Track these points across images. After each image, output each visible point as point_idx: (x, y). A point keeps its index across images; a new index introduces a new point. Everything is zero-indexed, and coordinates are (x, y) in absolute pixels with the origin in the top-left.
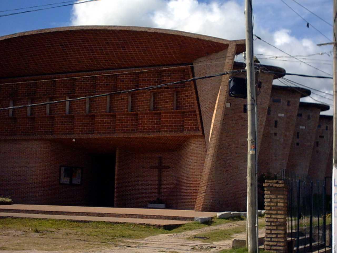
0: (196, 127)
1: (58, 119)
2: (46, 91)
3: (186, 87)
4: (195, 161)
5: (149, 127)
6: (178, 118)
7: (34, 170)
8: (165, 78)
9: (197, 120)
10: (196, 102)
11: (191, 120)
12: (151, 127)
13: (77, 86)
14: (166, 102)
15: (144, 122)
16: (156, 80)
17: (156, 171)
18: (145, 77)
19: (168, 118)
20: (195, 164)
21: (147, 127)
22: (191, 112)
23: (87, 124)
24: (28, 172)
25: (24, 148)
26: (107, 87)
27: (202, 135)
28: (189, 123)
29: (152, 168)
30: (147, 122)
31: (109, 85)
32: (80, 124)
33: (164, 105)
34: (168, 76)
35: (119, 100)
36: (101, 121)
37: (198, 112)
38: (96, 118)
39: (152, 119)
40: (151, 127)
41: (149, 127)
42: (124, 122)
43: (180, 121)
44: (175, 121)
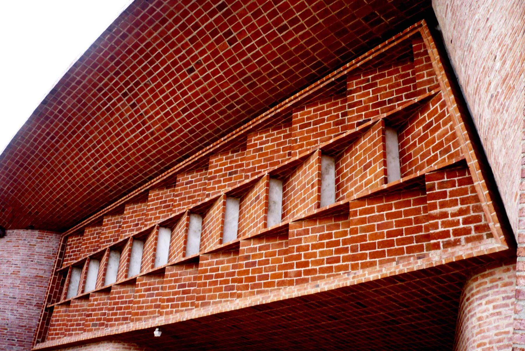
0: (477, 228)
5: (321, 262)
6: (407, 213)
8: (358, 97)
9: (476, 199)
10: (460, 127)
11: (454, 203)
12: (329, 261)
15: (307, 248)
16: (337, 116)
23: (190, 285)
27: (505, 247)
28: (444, 215)
30: (314, 247)
31: (236, 172)
33: (362, 178)
34: (365, 88)
37: (473, 163)
39: (330, 236)
40: (329, 261)
41: (321, 262)
42: (260, 263)
43: (417, 221)
44: (398, 224)
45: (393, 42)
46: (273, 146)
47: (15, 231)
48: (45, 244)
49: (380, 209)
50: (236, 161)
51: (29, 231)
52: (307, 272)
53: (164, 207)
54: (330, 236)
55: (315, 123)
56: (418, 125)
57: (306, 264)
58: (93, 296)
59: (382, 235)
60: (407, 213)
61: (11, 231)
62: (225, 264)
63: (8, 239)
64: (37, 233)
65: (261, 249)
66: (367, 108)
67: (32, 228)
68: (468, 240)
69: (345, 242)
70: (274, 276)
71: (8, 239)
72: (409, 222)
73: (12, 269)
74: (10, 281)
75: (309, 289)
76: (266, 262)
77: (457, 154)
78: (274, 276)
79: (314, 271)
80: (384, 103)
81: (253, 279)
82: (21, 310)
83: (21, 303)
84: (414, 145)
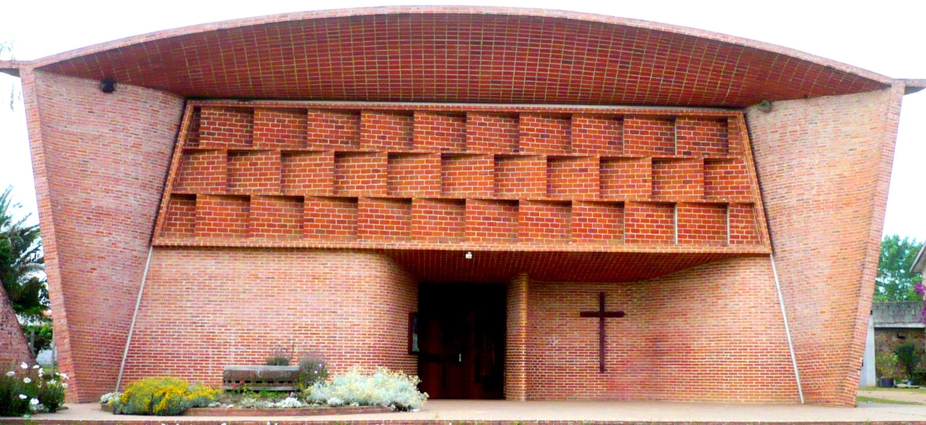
1: (420, 207)
2: (384, 138)
3: (732, 154)
4: (752, 304)
6: (709, 217)
11: (742, 222)
13: (471, 133)
15: (637, 221)
18: (637, 127)
19: (690, 216)
20: (753, 310)
21: (644, 231)
22: (743, 205)
23: (494, 219)
24: (339, 325)
25: (327, 270)
26: (543, 141)
29: (584, 315)
30: (643, 221)
31: (548, 136)
32: (479, 218)
33: (681, 187)
34: (689, 129)
35: (575, 170)
36: (532, 214)
37: (759, 207)
38: (522, 209)
42: (590, 220)
45: (720, 113)
46: (595, 132)
47: (130, 87)
48: (168, 111)
49: (695, 211)
50: (548, 126)
51: (151, 91)
52: (638, 236)
53: (437, 134)
54: (652, 216)
55: (642, 133)
56: (721, 168)
57: (638, 231)
58: (309, 200)
59: (695, 226)
60: (709, 217)
61: (122, 86)
62: (546, 213)
63: (120, 97)
64: (160, 94)
65: (590, 210)
66: (689, 143)
67: (155, 88)
68: (747, 242)
69: (662, 222)
70: (601, 231)
71: (120, 97)
72: (709, 222)
73: (132, 140)
74: (131, 156)
75: (647, 249)
76: (595, 220)
77: (749, 197)
78: (601, 231)
79: (642, 236)
80: (698, 144)
81: (585, 231)
82: (144, 195)
83: (144, 186)
84: (716, 178)
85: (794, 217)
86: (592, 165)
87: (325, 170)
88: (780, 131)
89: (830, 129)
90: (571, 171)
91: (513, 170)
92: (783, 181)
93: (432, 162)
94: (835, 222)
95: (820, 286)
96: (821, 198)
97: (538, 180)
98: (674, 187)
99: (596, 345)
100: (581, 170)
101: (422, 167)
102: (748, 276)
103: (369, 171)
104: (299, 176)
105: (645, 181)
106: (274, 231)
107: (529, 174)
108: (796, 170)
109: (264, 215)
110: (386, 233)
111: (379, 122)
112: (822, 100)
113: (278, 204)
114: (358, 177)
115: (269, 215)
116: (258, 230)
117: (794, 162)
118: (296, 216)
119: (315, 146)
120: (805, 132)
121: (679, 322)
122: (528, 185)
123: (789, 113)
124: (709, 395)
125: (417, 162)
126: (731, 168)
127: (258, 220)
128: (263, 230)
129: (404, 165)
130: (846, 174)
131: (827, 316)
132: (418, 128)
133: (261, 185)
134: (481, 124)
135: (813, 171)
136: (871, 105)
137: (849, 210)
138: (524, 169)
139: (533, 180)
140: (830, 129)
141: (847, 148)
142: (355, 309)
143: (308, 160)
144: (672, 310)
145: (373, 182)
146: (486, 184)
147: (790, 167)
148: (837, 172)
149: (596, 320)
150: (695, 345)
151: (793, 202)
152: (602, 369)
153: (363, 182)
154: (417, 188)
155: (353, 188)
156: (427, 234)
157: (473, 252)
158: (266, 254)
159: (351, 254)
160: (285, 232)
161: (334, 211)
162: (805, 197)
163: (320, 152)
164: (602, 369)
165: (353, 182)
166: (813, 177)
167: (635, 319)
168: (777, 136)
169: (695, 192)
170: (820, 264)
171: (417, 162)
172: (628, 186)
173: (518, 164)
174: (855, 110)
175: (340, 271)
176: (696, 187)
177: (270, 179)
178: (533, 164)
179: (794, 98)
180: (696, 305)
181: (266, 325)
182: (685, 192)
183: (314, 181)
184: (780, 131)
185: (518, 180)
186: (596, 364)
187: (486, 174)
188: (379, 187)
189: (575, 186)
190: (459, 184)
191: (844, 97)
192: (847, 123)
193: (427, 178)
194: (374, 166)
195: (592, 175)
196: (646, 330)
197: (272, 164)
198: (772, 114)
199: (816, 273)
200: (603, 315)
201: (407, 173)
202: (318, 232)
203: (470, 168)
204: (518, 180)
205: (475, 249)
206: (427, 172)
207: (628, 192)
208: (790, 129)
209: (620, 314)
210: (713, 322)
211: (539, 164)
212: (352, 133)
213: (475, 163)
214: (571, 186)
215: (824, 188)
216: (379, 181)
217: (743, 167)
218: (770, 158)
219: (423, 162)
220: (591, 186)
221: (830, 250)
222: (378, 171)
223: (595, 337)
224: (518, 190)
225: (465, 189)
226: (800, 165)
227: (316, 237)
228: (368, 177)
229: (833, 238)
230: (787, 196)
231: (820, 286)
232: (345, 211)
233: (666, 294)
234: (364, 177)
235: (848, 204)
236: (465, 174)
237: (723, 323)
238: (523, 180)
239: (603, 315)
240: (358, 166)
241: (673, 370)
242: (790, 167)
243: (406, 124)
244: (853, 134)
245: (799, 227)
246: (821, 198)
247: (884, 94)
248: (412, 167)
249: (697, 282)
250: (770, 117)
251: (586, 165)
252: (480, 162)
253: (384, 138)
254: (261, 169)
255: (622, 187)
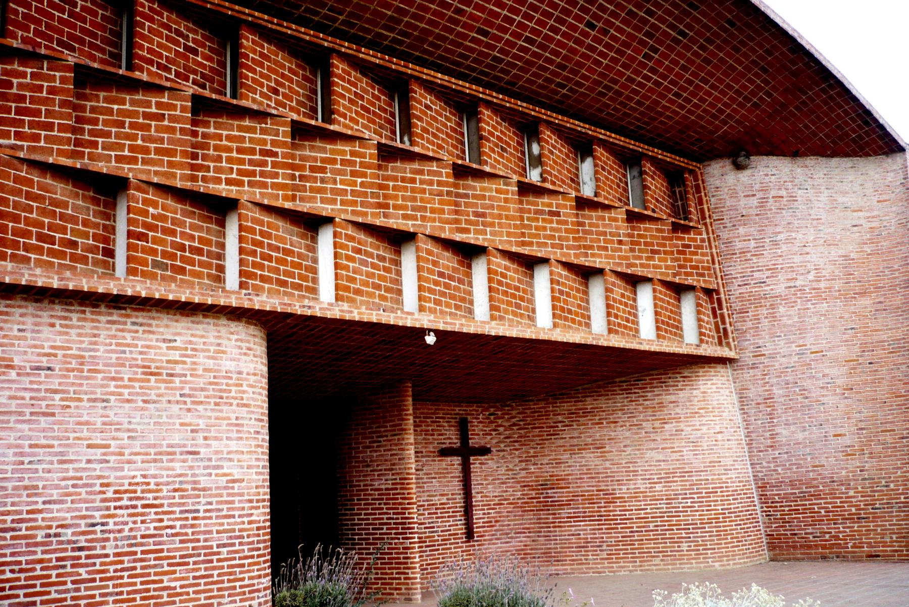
7: (237, 474)
14: (654, 252)
17: (457, 460)
20: (719, 437)
24: (204, 482)
25: (175, 355)
29: (445, 453)
35: (541, 212)
58: (138, 189)
77: (710, 282)
85: (782, 309)
86: (565, 207)
87: (172, 130)
88: (760, 195)
89: (824, 198)
90: (537, 212)
91: (466, 196)
92: (762, 262)
93: (363, 155)
94: (847, 316)
95: (830, 400)
96: (822, 285)
97: (507, 217)
98: (640, 258)
99: (459, 499)
100: (551, 213)
101: (343, 162)
102: (714, 390)
103: (252, 151)
104: (108, 135)
105: (620, 242)
106: (51, 253)
107: (492, 207)
108: (784, 247)
109: (30, 209)
110: (284, 284)
111: (267, 58)
112: (810, 161)
113: (60, 190)
114: (230, 160)
115: (43, 212)
116: (15, 245)
117: (781, 237)
118: (96, 226)
119: (150, 73)
120: (793, 199)
121: (590, 459)
122: (492, 225)
123: (771, 173)
124: (657, 561)
125: (333, 152)
126: (690, 239)
127: (16, 219)
128: (27, 248)
129: (308, 153)
130: (852, 255)
131: (847, 440)
132: (340, 86)
133: (19, 136)
134: (427, 107)
135: (807, 250)
136: (871, 173)
137: (866, 302)
138: (483, 197)
139: (500, 217)
140: (824, 198)
141: (848, 223)
142: (234, 445)
143: (128, 102)
144: (575, 441)
145: (262, 174)
146: (442, 211)
147: (775, 243)
148: (841, 252)
149: (457, 460)
150: (623, 491)
151: (780, 289)
152: (470, 534)
153: (241, 172)
154: (334, 202)
155: (218, 181)
156: (358, 292)
157: (437, 332)
158: (31, 308)
159: (223, 321)
160: (74, 258)
161: (182, 224)
162: (798, 283)
163: (160, 89)
164: (470, 534)
165: (218, 170)
166: (808, 258)
167: (503, 457)
168: (754, 202)
169: (667, 267)
170: (827, 371)
171: (333, 152)
172: (599, 248)
173: (474, 188)
174: (851, 178)
175: (201, 359)
176: (665, 260)
177: (49, 127)
178: (497, 191)
179: (784, 155)
180: (623, 433)
181: (32, 490)
182: (655, 267)
183: (146, 151)
184: (760, 195)
185: (477, 214)
186: (460, 529)
187: (440, 194)
188: (275, 186)
189: (545, 237)
190: (395, 207)
191: (835, 161)
192: (844, 193)
193: (354, 184)
194: (264, 142)
195: (566, 223)
196: (523, 473)
197: (52, 91)
198: (747, 172)
199: (820, 383)
200: (466, 452)
201: (313, 169)
202: (156, 264)
203: (413, 181)
204: (477, 214)
205: (441, 327)
206: (354, 174)
207: (600, 256)
208: (773, 193)
209: (484, 451)
210: (649, 454)
211: (507, 192)
212: (212, 69)
213: (421, 172)
214: (537, 236)
215: (824, 273)
216: (276, 176)
217: (703, 240)
218: (742, 230)
219: (343, 153)
220: (567, 239)
221: (842, 352)
222: (275, 154)
223: (455, 486)
224: (477, 232)
225: (405, 217)
226: (790, 241)
227: (153, 276)
228: (251, 163)
229: (845, 337)
230: (769, 281)
231: (830, 400)
232: (200, 229)
233: (560, 418)
234: (241, 162)
235: (863, 294)
236: (405, 189)
237: (675, 456)
238: (483, 215)
239: (466, 452)
240: (229, 138)
241: (585, 529)
242: (775, 243)
243: (305, 78)
244: (855, 207)
245: (789, 322)
246: (822, 285)
247: (890, 160)
248: (323, 160)
249: (620, 400)
250: (744, 176)
251: (558, 206)
252: (430, 173)
253: (276, 92)
254: (21, 98)
255: (591, 248)
